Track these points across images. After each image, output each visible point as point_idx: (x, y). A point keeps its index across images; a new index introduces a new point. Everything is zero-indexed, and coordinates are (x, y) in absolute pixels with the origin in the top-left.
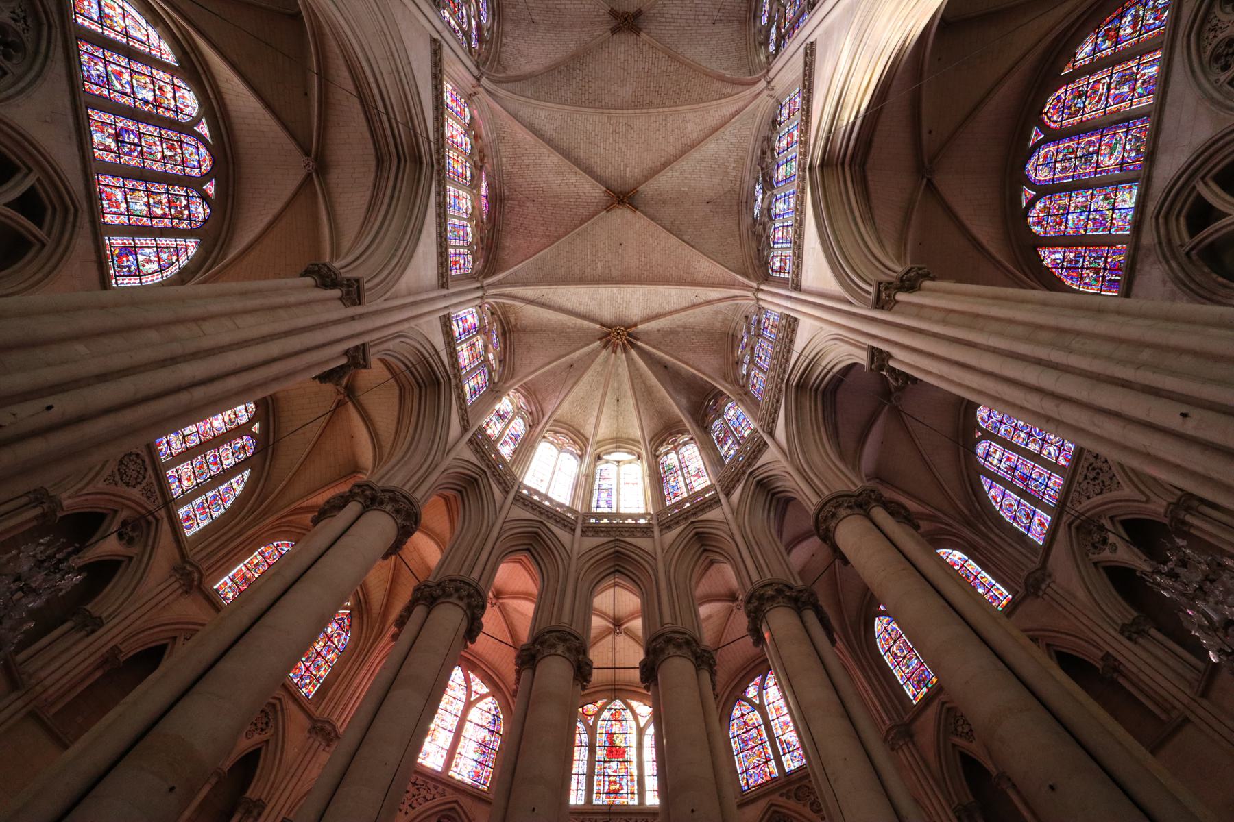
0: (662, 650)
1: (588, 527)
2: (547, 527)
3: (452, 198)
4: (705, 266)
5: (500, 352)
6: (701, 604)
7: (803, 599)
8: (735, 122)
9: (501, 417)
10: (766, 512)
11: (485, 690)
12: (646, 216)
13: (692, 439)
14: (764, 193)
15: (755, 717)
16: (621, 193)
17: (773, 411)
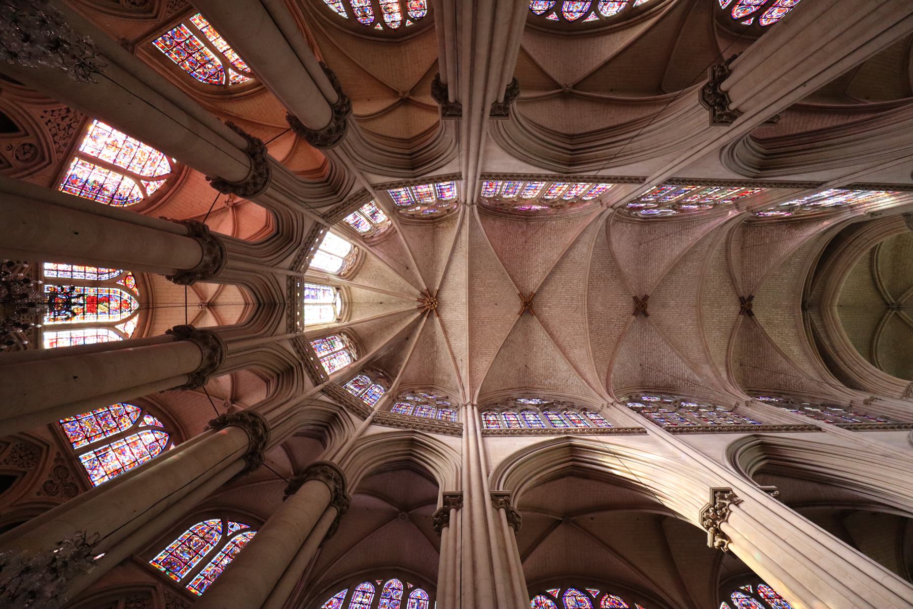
0: (206, 344)
1: (294, 281)
2: (296, 248)
3: (536, 185)
4: (484, 365)
5: (420, 215)
6: (232, 375)
7: (254, 459)
8: (582, 382)
9: (373, 215)
10: (314, 422)
11: (149, 192)
12: (517, 322)
13: (354, 360)
14: (538, 405)
15: (127, 425)
16: (532, 304)
17: (391, 422)
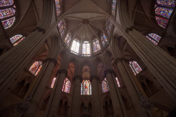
4: (101, 10)
11: (67, 80)
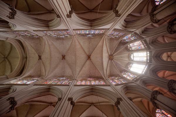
4: (100, 44)
